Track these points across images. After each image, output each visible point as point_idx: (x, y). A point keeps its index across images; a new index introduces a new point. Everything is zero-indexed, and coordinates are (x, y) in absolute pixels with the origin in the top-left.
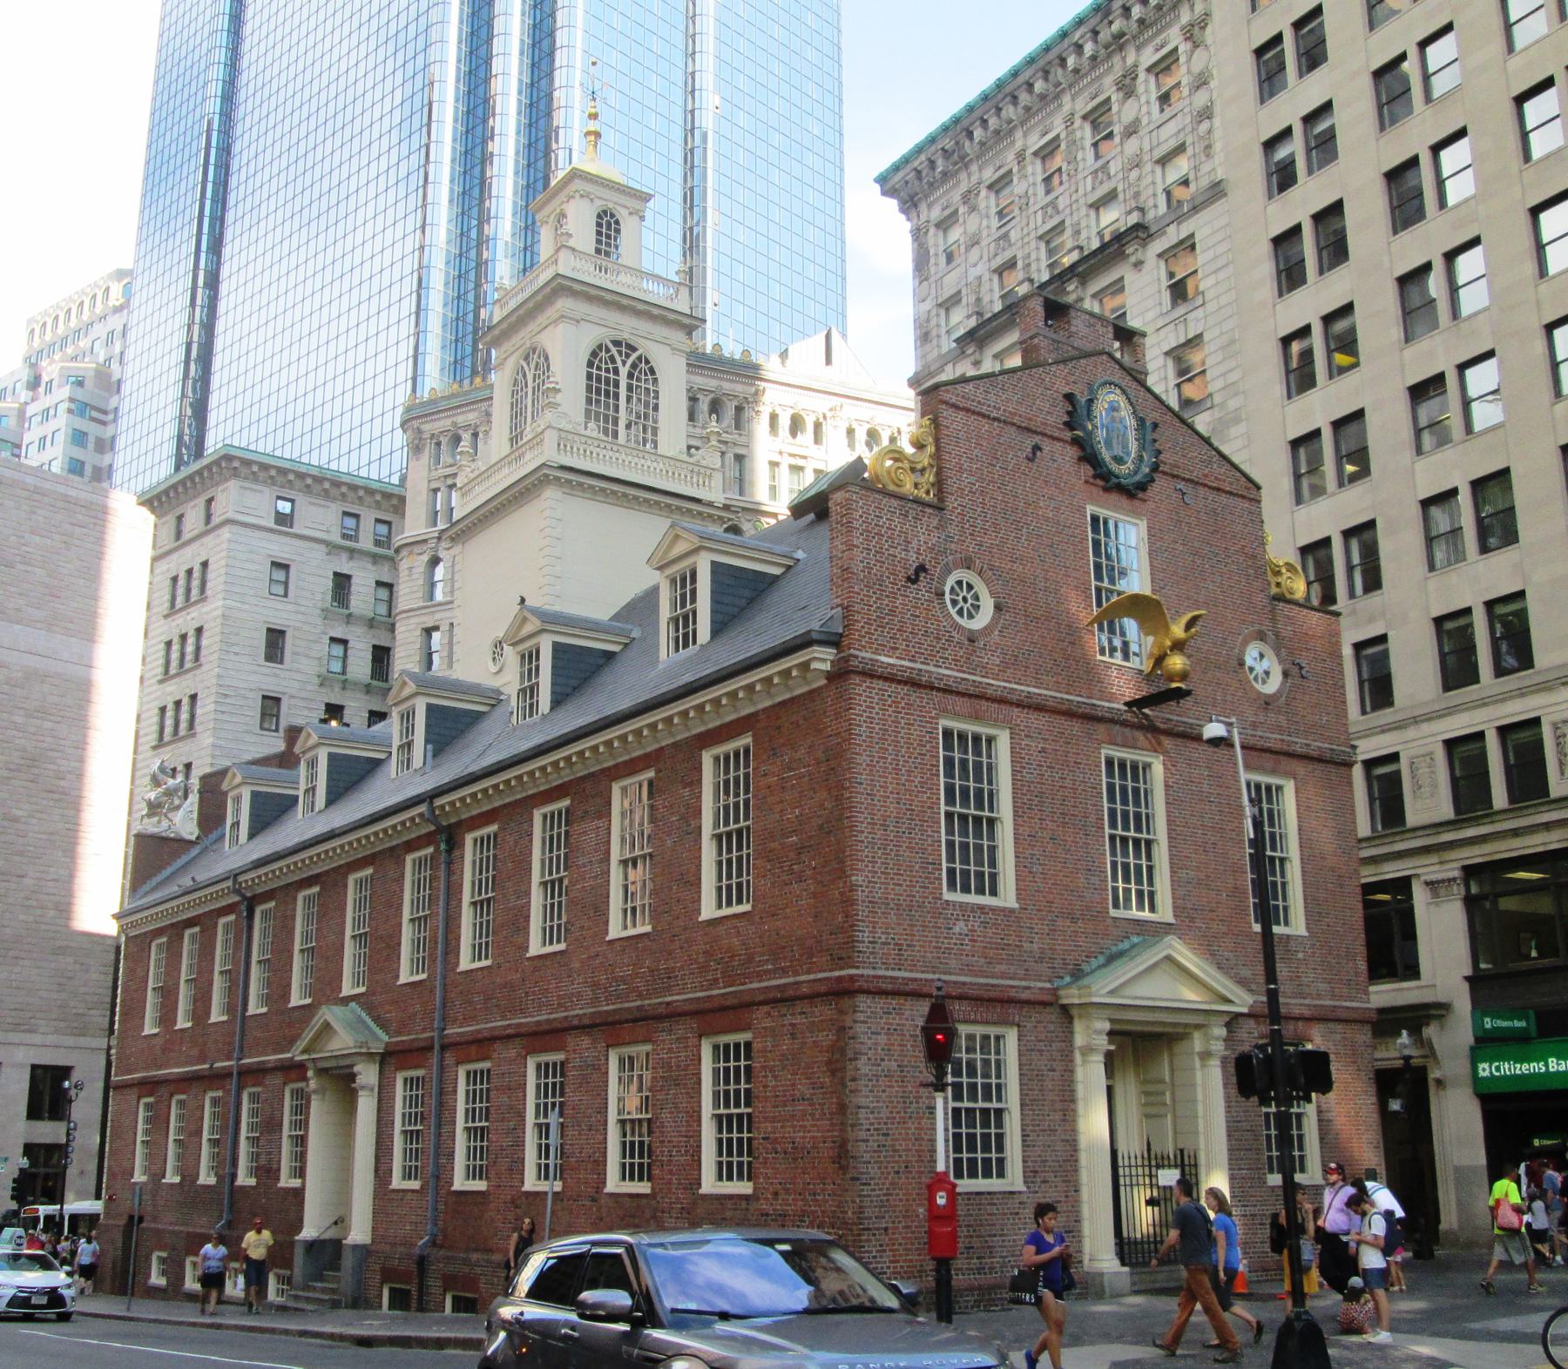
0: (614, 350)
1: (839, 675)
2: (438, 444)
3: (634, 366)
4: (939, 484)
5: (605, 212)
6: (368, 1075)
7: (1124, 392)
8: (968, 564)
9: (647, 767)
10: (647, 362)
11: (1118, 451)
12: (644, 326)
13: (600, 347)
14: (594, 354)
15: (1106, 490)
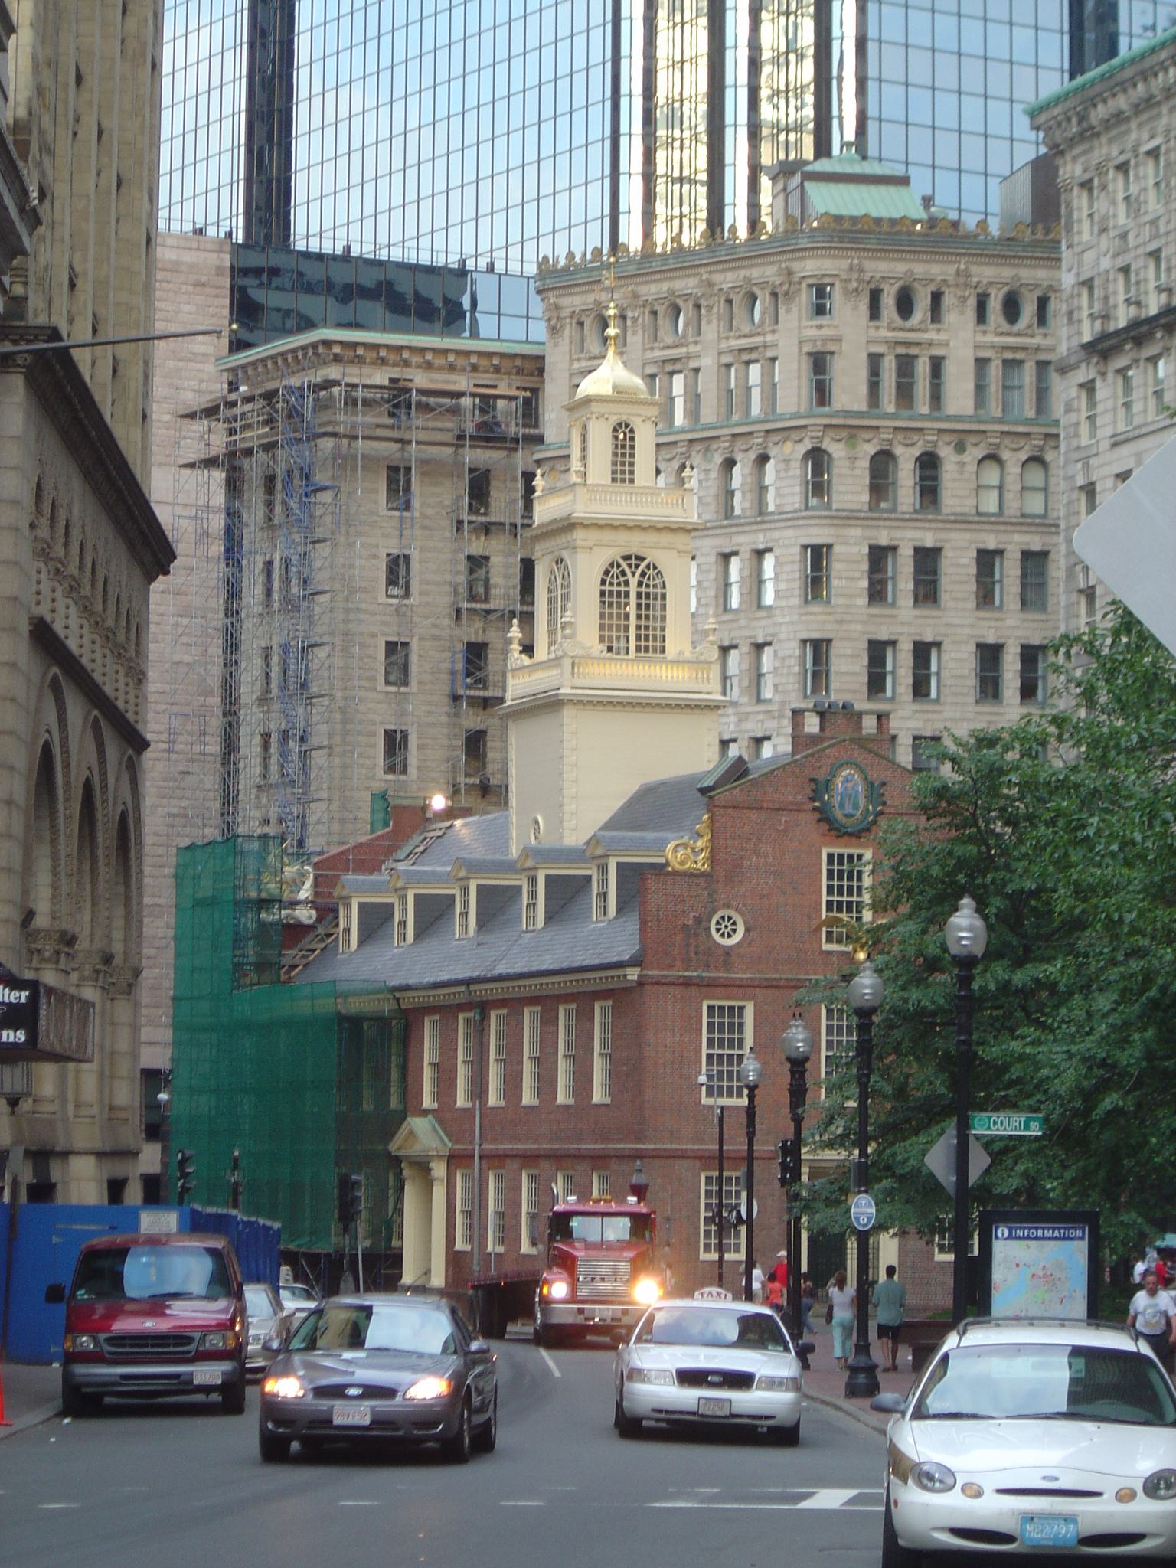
0: (624, 565)
1: (641, 983)
2: (581, 324)
3: (643, 574)
4: (712, 859)
5: (620, 425)
6: (439, 1170)
7: (857, 766)
8: (728, 906)
9: (573, 1001)
10: (655, 568)
11: (849, 809)
12: (651, 538)
13: (612, 564)
14: (607, 573)
15: (838, 837)
